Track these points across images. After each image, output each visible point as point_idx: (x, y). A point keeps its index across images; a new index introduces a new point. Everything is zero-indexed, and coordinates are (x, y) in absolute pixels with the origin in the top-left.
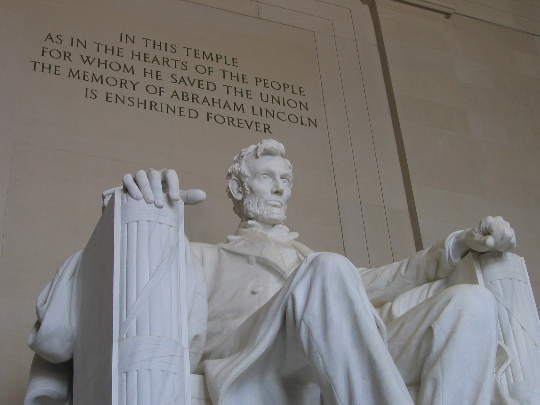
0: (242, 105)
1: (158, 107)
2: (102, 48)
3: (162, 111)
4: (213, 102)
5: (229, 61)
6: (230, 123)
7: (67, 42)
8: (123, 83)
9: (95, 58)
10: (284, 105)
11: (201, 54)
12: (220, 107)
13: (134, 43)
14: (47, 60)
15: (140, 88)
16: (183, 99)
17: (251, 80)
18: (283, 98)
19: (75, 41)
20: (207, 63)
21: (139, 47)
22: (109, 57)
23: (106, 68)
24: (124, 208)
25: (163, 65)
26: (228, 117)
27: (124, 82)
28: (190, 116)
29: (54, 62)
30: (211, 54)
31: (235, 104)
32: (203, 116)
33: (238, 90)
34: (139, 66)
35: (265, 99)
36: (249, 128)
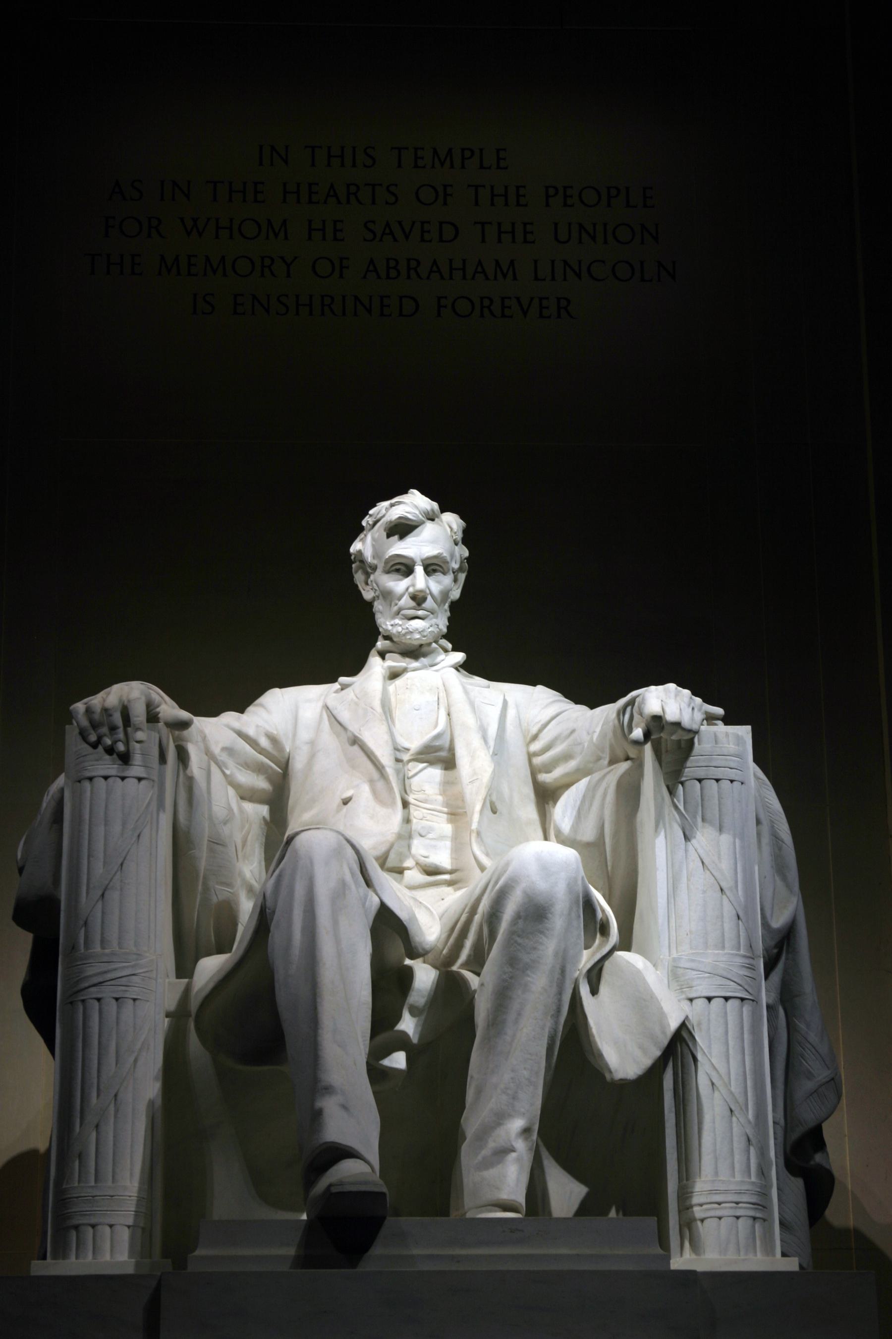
0: (512, 263)
3: (344, 314)
4: (451, 269)
6: (486, 311)
9: (209, 219)
10: (606, 242)
12: (464, 278)
13: (286, 162)
16: (388, 277)
18: (605, 225)
23: (231, 237)
25: (348, 202)
26: (482, 298)
27: (267, 262)
28: (401, 315)
30: (450, 150)
31: (497, 263)
36: (525, 313)
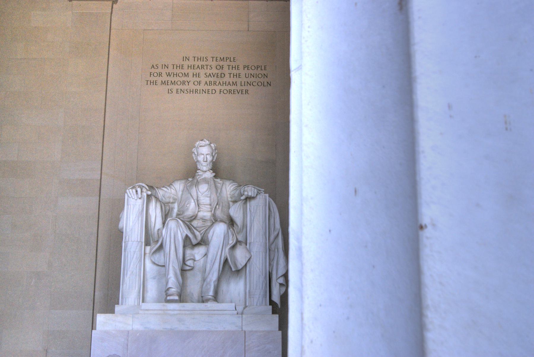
1: (198, 92)
2: (175, 66)
5: (232, 60)
7: (160, 67)
8: (183, 83)
11: (219, 58)
14: (153, 79)
15: (191, 84)
17: (241, 67)
19: (164, 66)
20: (221, 63)
21: (191, 62)
22: (178, 71)
24: (128, 200)
29: (155, 79)
32: (218, 91)
33: (235, 74)
34: (191, 72)
35: (247, 76)
